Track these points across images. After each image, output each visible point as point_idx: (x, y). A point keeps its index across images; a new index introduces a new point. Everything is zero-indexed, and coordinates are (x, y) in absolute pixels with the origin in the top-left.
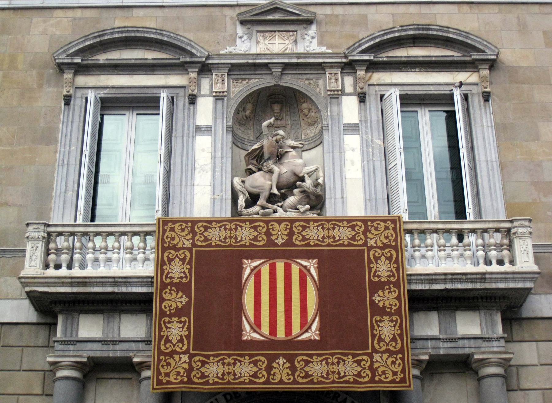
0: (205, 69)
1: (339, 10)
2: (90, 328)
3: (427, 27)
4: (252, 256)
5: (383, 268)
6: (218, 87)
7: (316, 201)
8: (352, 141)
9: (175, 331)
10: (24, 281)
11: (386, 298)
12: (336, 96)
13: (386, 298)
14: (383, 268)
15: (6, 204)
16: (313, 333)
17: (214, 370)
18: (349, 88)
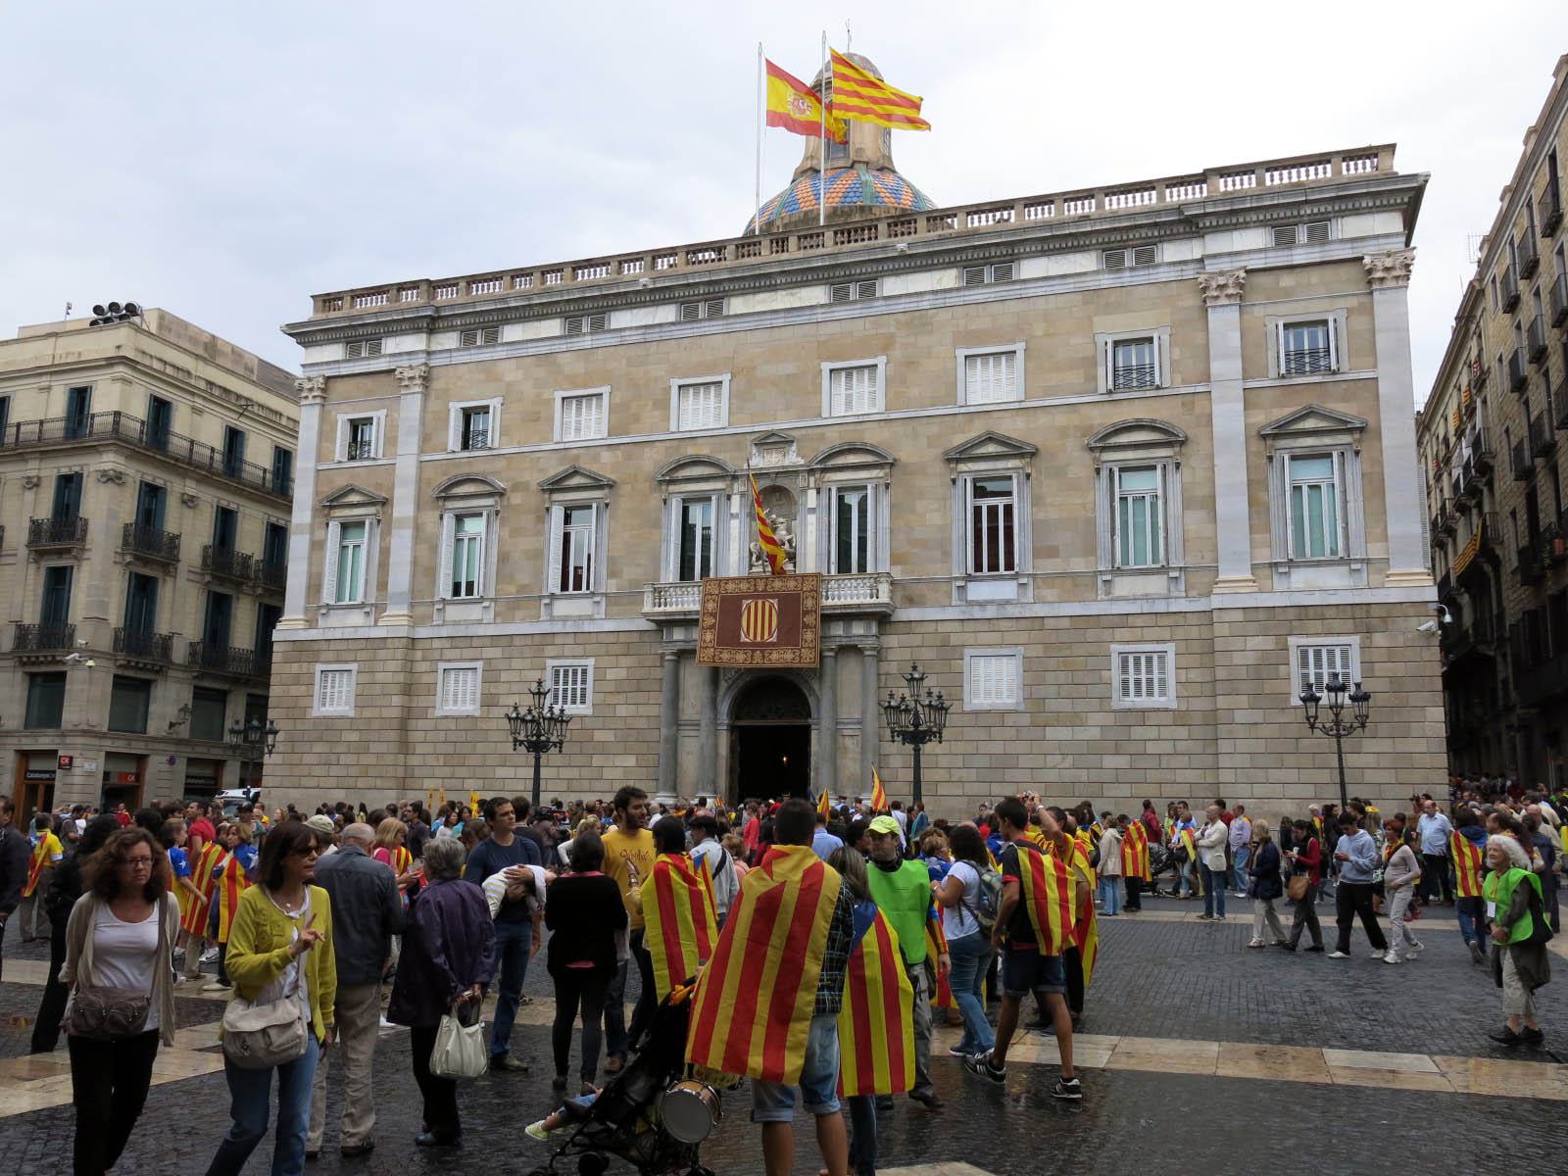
0: (735, 478)
1: (810, 431)
2: (678, 634)
3: (854, 443)
4: (747, 598)
5: (809, 603)
6: (743, 489)
8: (812, 519)
9: (708, 636)
10: (645, 615)
11: (809, 619)
12: (804, 490)
13: (809, 619)
14: (809, 603)
15: (638, 565)
16: (774, 639)
17: (725, 656)
18: (812, 485)
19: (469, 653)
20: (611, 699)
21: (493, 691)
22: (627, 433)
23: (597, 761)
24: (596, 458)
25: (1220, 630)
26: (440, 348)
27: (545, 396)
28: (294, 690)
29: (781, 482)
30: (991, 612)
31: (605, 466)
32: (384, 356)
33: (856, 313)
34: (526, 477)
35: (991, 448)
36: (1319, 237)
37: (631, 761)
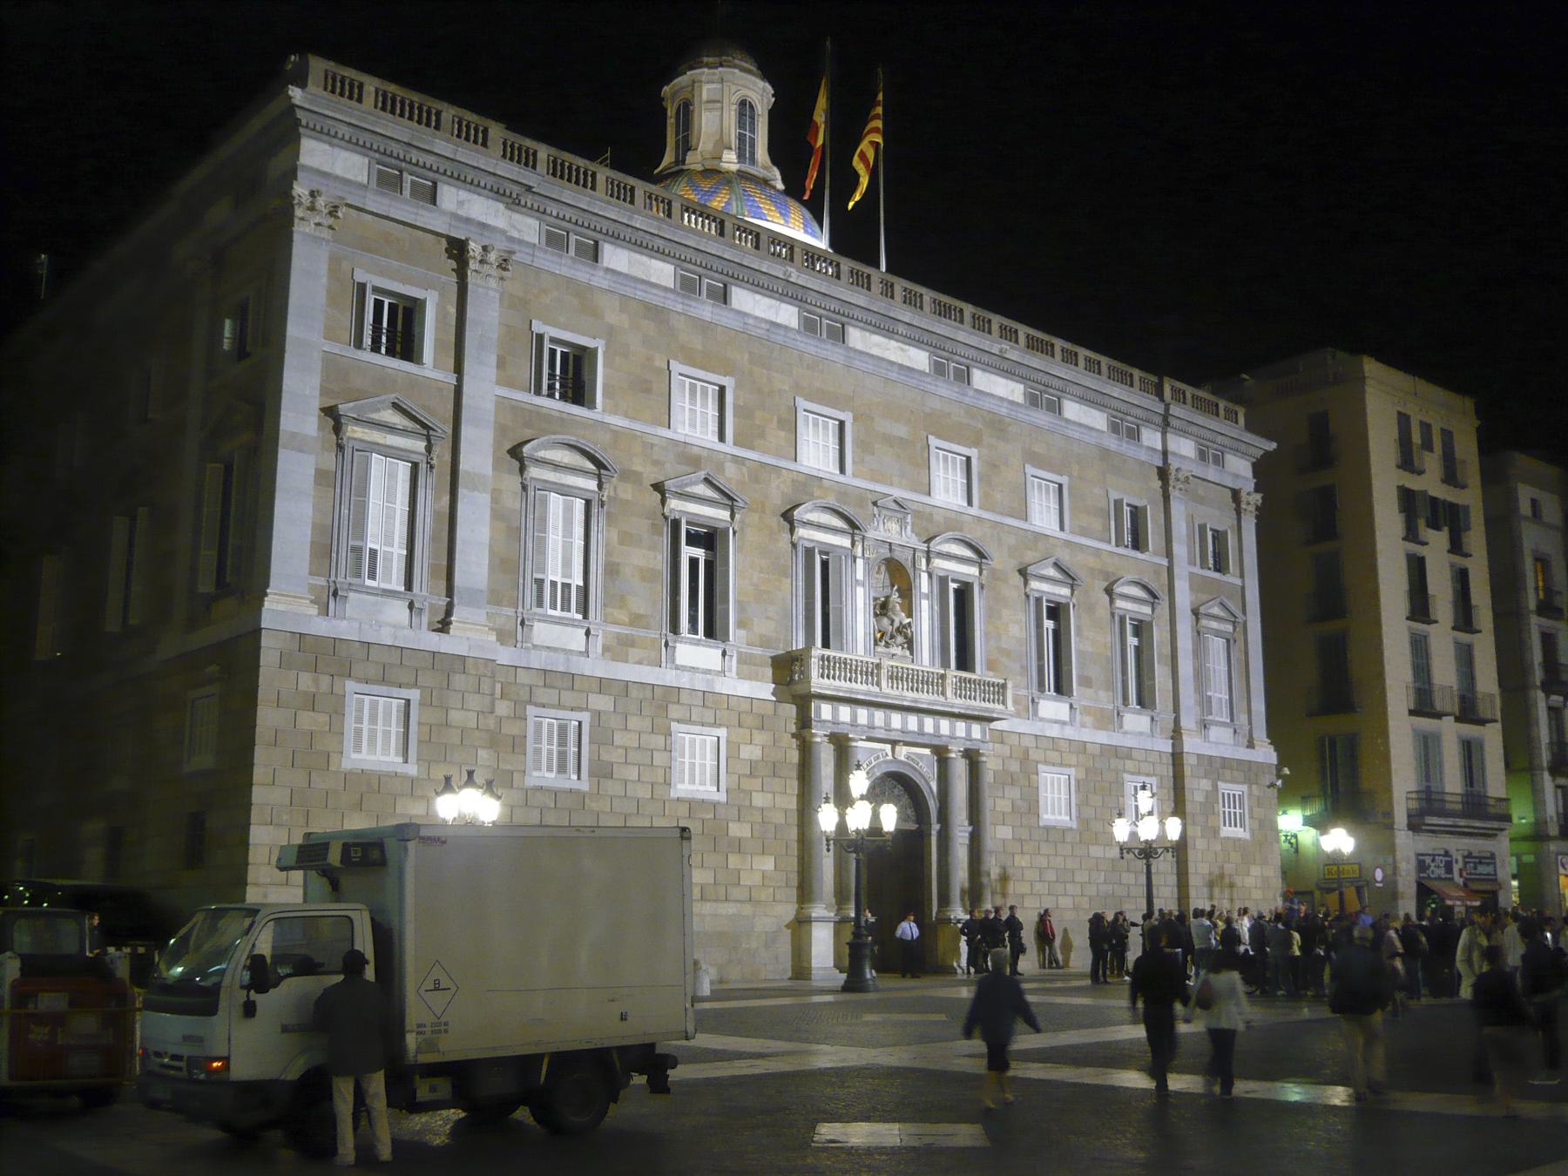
2: (826, 711)
7: (910, 644)
19: (568, 697)
20: (747, 784)
21: (605, 757)
22: (752, 448)
23: (734, 861)
24: (720, 467)
25: (1187, 771)
26: (515, 234)
27: (657, 363)
28: (307, 720)
29: (899, 555)
30: (1054, 731)
31: (730, 477)
32: (444, 213)
33: (954, 396)
34: (637, 467)
35: (1051, 572)
36: (1219, 461)
37: (768, 864)
